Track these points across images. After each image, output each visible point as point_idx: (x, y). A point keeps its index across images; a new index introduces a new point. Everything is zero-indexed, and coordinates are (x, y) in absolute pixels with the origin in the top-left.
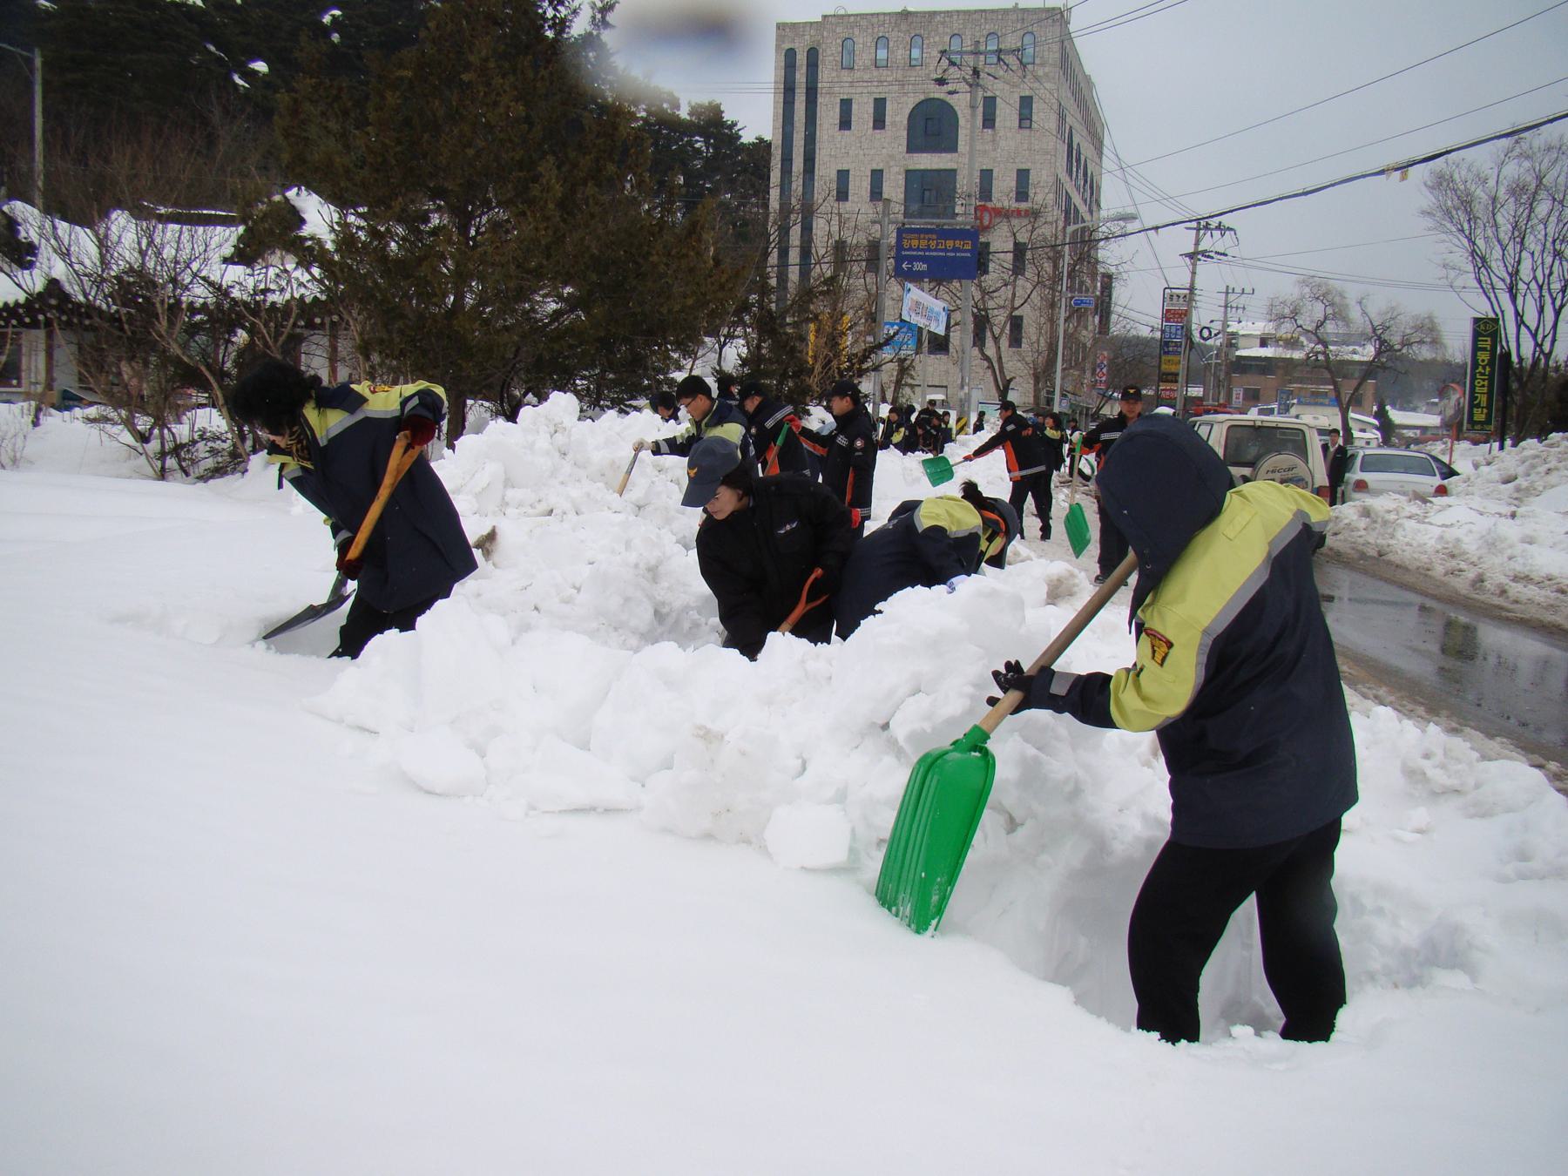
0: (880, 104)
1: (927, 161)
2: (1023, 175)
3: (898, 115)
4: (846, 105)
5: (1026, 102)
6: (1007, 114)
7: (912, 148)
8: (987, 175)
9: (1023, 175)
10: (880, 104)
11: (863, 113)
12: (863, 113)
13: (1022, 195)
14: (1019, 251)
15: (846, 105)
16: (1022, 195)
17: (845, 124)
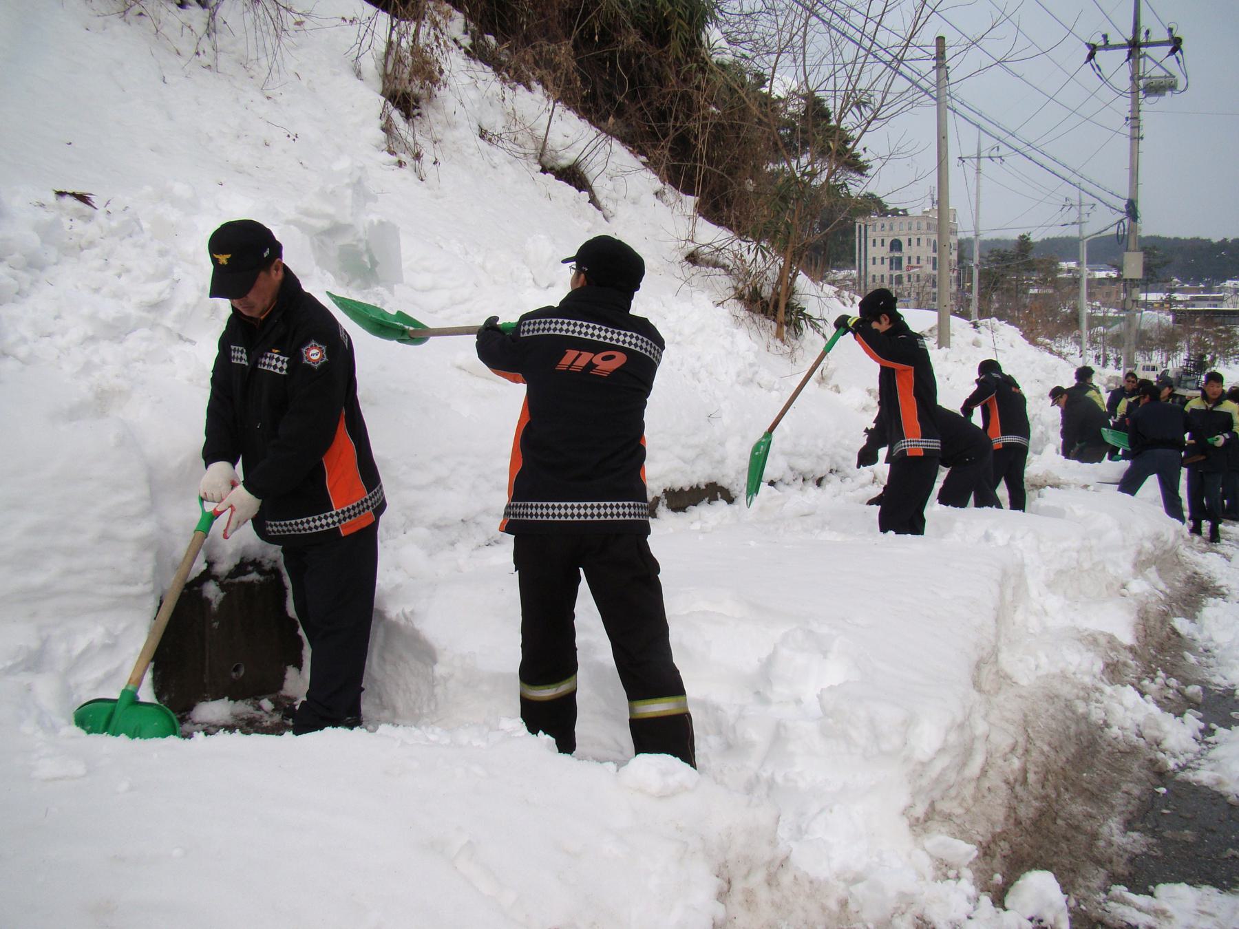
0: (883, 241)
1: (897, 254)
2: (918, 258)
3: (887, 243)
4: (874, 241)
5: (919, 240)
6: (914, 242)
7: (891, 250)
8: (909, 258)
9: (918, 258)
10: (883, 241)
11: (878, 242)
12: (878, 242)
13: (918, 263)
14: (918, 276)
15: (874, 241)
16: (918, 263)
17: (874, 245)
